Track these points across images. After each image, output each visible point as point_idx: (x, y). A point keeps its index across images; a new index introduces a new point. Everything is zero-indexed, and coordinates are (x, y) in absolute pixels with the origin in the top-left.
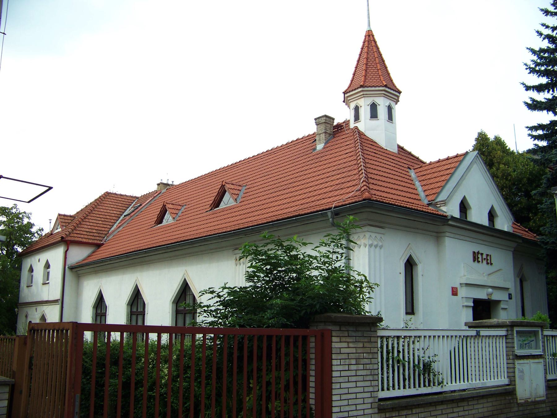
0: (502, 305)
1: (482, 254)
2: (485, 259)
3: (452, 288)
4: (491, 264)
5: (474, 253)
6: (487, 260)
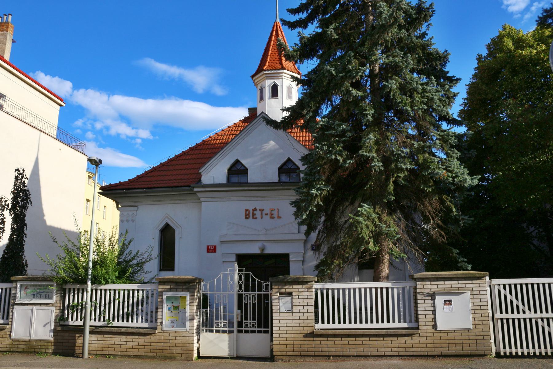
0: (292, 258)
1: (262, 210)
2: (267, 214)
3: (208, 247)
4: (279, 217)
5: (246, 210)
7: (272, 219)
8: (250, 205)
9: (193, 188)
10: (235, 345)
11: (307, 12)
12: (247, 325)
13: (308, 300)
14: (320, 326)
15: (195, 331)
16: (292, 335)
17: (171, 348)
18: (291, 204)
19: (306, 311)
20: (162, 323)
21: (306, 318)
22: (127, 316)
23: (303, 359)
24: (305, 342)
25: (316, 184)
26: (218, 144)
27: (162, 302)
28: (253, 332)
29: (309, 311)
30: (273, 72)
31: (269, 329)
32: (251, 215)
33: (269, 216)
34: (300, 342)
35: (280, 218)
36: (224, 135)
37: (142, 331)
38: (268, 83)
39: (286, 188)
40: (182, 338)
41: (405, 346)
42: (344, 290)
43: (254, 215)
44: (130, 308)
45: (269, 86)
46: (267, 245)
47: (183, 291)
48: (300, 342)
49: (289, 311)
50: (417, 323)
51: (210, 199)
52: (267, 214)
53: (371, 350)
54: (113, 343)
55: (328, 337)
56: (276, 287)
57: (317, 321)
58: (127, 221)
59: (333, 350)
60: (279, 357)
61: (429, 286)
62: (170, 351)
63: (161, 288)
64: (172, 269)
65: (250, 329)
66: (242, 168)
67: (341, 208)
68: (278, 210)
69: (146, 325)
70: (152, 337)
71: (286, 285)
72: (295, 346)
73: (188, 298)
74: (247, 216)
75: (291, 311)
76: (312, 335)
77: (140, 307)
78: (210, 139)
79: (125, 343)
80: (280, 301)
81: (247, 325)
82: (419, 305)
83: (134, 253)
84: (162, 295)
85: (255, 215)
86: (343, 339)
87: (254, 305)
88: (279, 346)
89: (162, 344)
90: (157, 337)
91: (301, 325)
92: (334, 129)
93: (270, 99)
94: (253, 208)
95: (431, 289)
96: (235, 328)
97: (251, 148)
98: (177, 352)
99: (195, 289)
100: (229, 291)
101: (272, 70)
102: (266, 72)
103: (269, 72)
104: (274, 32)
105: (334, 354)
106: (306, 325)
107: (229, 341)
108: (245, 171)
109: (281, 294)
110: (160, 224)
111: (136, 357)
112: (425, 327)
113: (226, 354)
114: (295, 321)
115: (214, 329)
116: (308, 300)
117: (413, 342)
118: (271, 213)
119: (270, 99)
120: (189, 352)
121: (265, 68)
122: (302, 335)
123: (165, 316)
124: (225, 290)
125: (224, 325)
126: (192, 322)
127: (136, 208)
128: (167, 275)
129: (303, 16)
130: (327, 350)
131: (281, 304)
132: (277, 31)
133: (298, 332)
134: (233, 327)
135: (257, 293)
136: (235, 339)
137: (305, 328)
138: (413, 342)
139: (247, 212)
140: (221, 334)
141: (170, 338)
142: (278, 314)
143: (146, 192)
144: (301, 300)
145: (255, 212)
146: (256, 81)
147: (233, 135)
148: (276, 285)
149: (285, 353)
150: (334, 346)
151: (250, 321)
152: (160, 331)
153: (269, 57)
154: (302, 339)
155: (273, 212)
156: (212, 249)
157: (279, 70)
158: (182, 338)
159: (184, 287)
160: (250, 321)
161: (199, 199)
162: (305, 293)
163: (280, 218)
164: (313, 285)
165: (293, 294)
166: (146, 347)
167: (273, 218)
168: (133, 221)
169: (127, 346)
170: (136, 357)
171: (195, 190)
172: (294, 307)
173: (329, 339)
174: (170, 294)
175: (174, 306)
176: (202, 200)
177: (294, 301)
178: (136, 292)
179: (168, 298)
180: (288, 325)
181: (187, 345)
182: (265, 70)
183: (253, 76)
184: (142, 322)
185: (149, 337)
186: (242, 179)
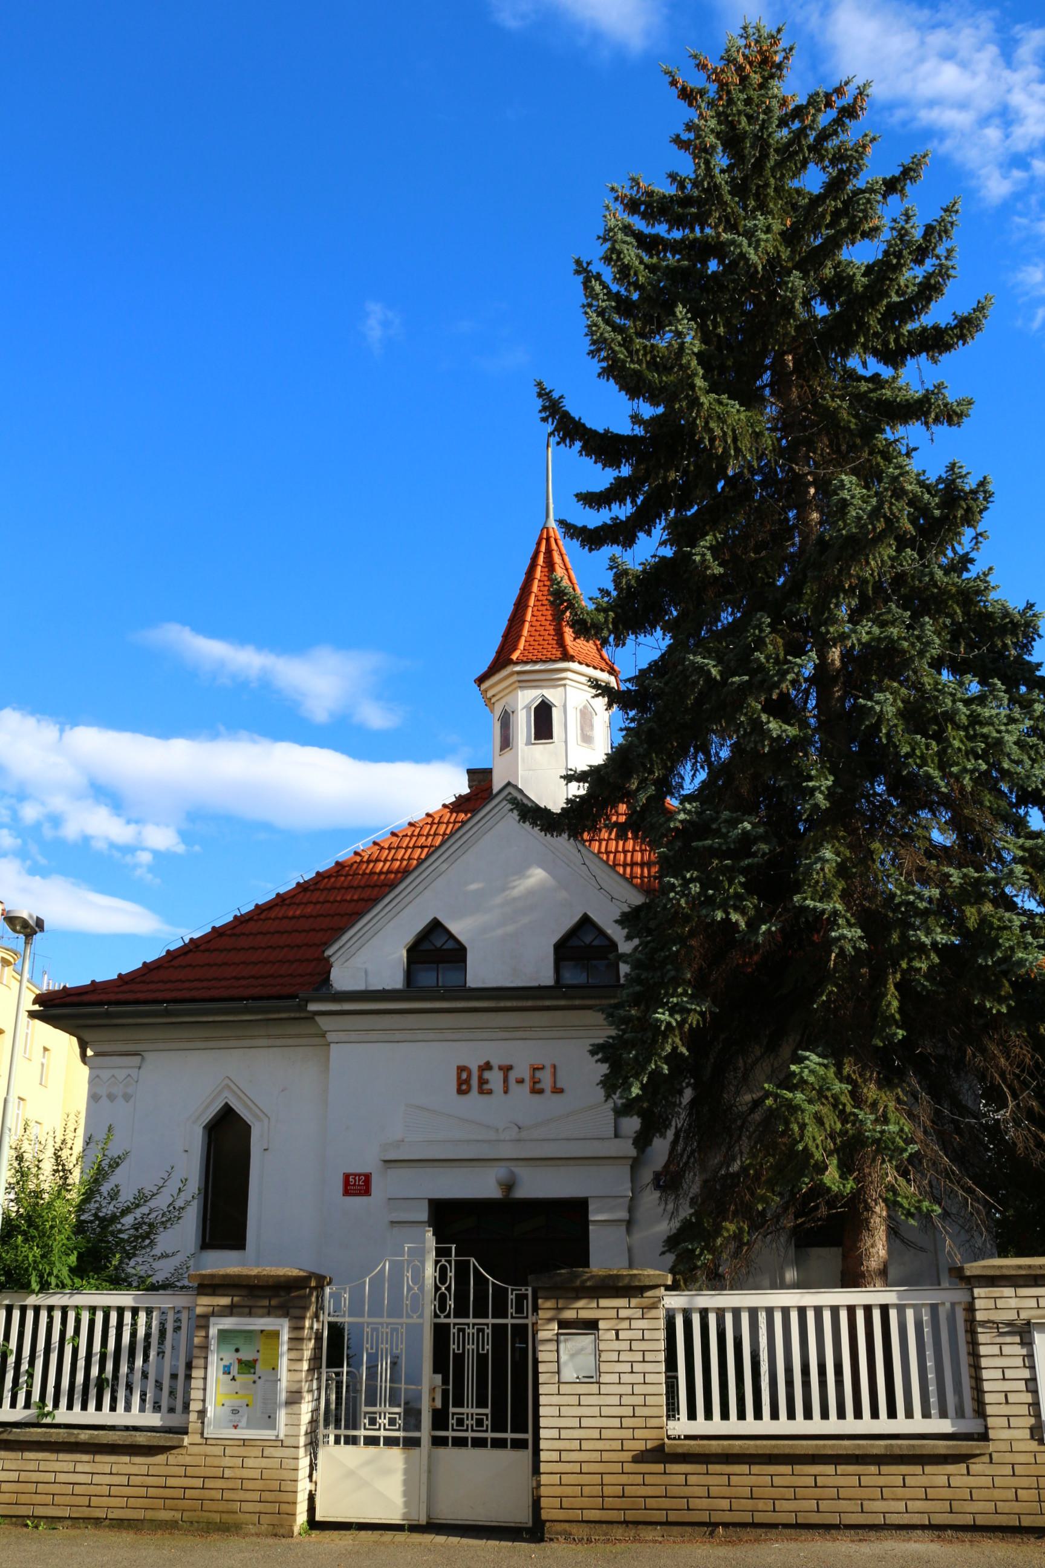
1: (506, 1069)
2: (520, 1081)
3: (347, 1177)
5: (461, 1069)
6: (535, 1082)
7: (537, 1096)
8: (472, 1054)
9: (307, 1001)
10: (424, 1484)
11: (633, 502)
12: (460, 1422)
13: (644, 1346)
14: (681, 1426)
15: (302, 1441)
16: (596, 1456)
17: (228, 1495)
18: (593, 1053)
19: (639, 1378)
20: (202, 1413)
21: (640, 1400)
22: (100, 1389)
23: (632, 1532)
24: (639, 1479)
25: (666, 994)
26: (381, 872)
27: (205, 1347)
28: (479, 1443)
29: (649, 1378)
30: (537, 667)
31: (529, 1436)
32: (475, 1082)
33: (527, 1086)
34: (624, 1479)
35: (561, 1091)
36: (398, 847)
37: (141, 1438)
38: (526, 699)
39: (577, 1002)
40: (264, 1463)
41: (947, 1493)
42: (753, 1312)
43: (482, 1082)
44: (109, 1366)
45: (528, 707)
46: (523, 1173)
47: (268, 1314)
48: (624, 1479)
49: (588, 1380)
50: (980, 1421)
51: (354, 1036)
52: (520, 1081)
53: (843, 1505)
54: (51, 1477)
55: (707, 1463)
56: (549, 1304)
57: (672, 1410)
58: (111, 1097)
59: (725, 1504)
60: (559, 1527)
61: (1013, 1303)
62: (222, 1506)
63: (204, 1303)
64: (239, 1243)
65: (470, 1434)
66: (450, 945)
67: (741, 1064)
68: (554, 1067)
69: (154, 1419)
70: (172, 1458)
71: (578, 1298)
72: (608, 1490)
73: (285, 1336)
74: (463, 1087)
75: (594, 1379)
76: (659, 1454)
77: (139, 1362)
78: (358, 859)
79: (87, 1479)
80: (562, 1346)
81: (460, 1422)
82: (984, 1362)
83: (126, 1197)
84: (206, 1327)
85: (487, 1082)
86: (756, 1469)
87: (482, 1359)
88: (559, 1491)
89: (198, 1483)
90: (188, 1460)
91: (627, 1422)
92: (717, 833)
93: (528, 743)
94: (482, 1063)
95: (1018, 1310)
96: (425, 1433)
97: (473, 887)
98: (246, 1507)
99: (306, 1308)
100: (408, 1316)
101: (535, 662)
102: (518, 668)
103: (528, 667)
104: (541, 557)
105: (728, 1517)
106: (640, 1422)
107: (406, 1472)
108: (457, 954)
109: (563, 1324)
110: (207, 1107)
111: (120, 1524)
112: (1006, 1434)
113: (395, 1517)
114: (605, 1411)
115: (362, 1433)
116: (644, 1346)
117: (971, 1481)
118: (533, 1077)
119: (528, 743)
120: (285, 1508)
121: (514, 657)
122: (627, 1456)
123: (215, 1390)
124: (395, 1310)
125: (392, 1422)
126: (295, 1407)
127: (139, 1058)
128: (224, 1263)
129: (623, 511)
130: (705, 1503)
131: (564, 1358)
132: (549, 552)
133: (617, 1445)
134: (418, 1428)
135: (490, 1321)
136: (425, 1468)
137: (638, 1434)
138: (971, 1481)
139: (464, 1076)
140: (381, 1450)
141: (227, 1461)
142: (554, 1389)
143: (167, 1013)
144: (625, 1345)
145: (487, 1075)
146: (489, 694)
147: (422, 847)
148: (547, 1298)
149: (577, 1515)
150: (727, 1492)
151: (470, 1410)
152: (197, 1439)
153: (527, 625)
154: (629, 1467)
155: (538, 1074)
156: (357, 1185)
157: (555, 661)
158: (264, 1463)
159: (274, 1302)
160: (470, 1410)
161: (323, 1035)
162: (636, 1324)
163: (561, 1091)
164: (660, 1299)
165: (602, 1325)
166: (152, 1492)
167: (541, 1092)
168: (127, 1097)
169: (93, 1490)
170: (120, 1524)
171: (313, 1007)
172: (604, 1367)
173: (712, 1468)
174: (228, 1323)
175: (240, 1361)
176: (330, 1037)
177: (603, 1346)
178: (128, 1317)
179: (223, 1335)
180: (585, 1422)
181: (275, 1485)
182: (517, 663)
183: (481, 680)
184: (142, 1409)
185: (160, 1458)
186: (449, 978)
